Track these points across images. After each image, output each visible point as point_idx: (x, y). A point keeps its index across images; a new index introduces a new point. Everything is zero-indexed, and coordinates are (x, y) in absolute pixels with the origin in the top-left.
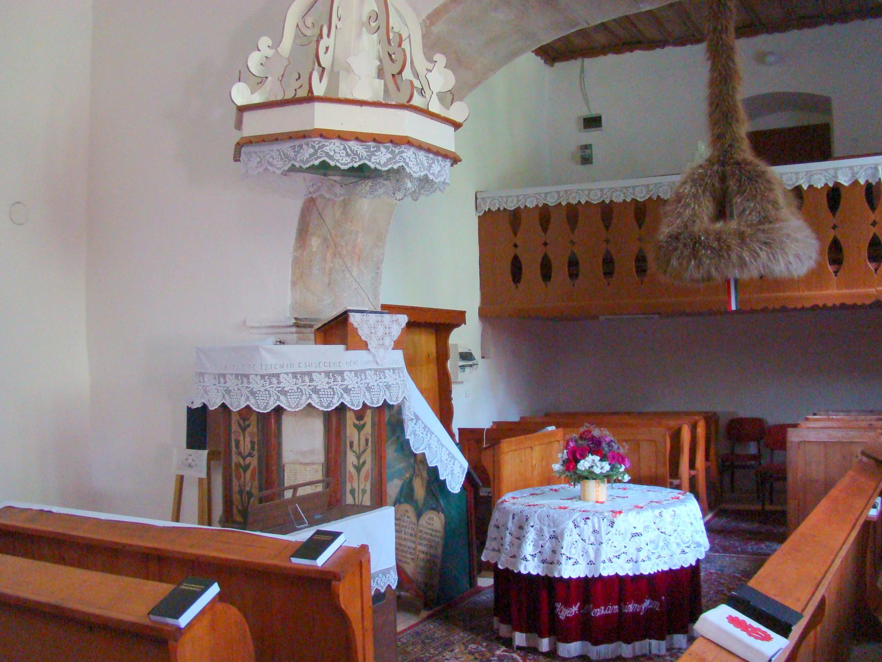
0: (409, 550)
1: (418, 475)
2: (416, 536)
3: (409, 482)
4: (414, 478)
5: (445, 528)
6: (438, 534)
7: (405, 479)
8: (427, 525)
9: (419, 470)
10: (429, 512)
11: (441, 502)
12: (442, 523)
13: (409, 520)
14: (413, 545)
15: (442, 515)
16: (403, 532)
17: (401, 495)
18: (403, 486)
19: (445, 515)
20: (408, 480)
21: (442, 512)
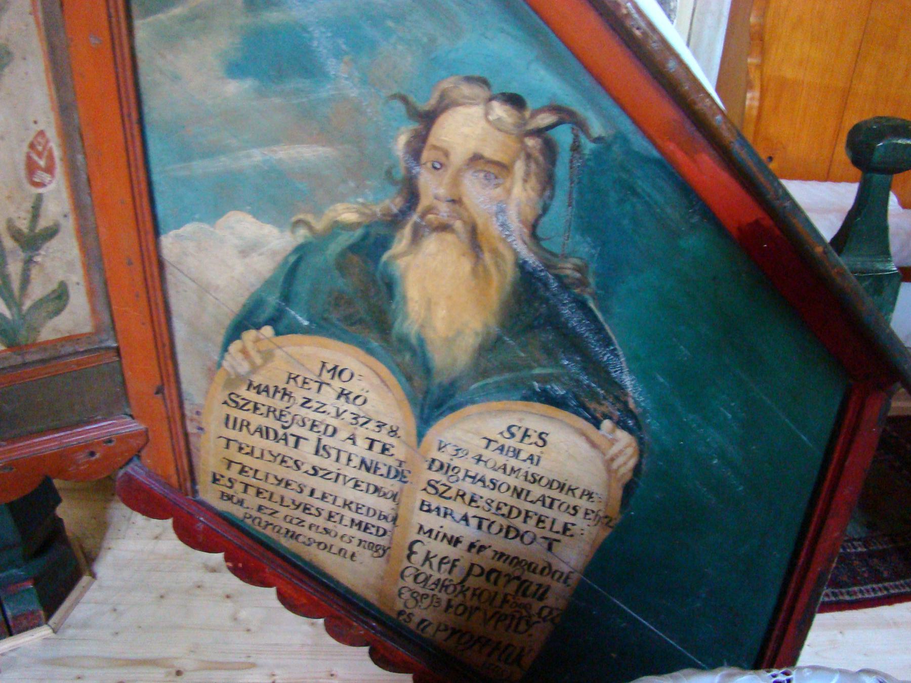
0: (349, 515)
1: (444, 228)
2: (400, 475)
3: (353, 248)
4: (407, 231)
5: (629, 489)
6: (583, 504)
7: (320, 225)
8: (501, 459)
9: (456, 201)
10: (521, 405)
11: (628, 381)
12: (609, 471)
13: (352, 408)
14: (385, 506)
15: (624, 438)
16: (307, 448)
17: (286, 298)
18: (302, 252)
19: (640, 441)
20: (345, 240)
21: (621, 424)
